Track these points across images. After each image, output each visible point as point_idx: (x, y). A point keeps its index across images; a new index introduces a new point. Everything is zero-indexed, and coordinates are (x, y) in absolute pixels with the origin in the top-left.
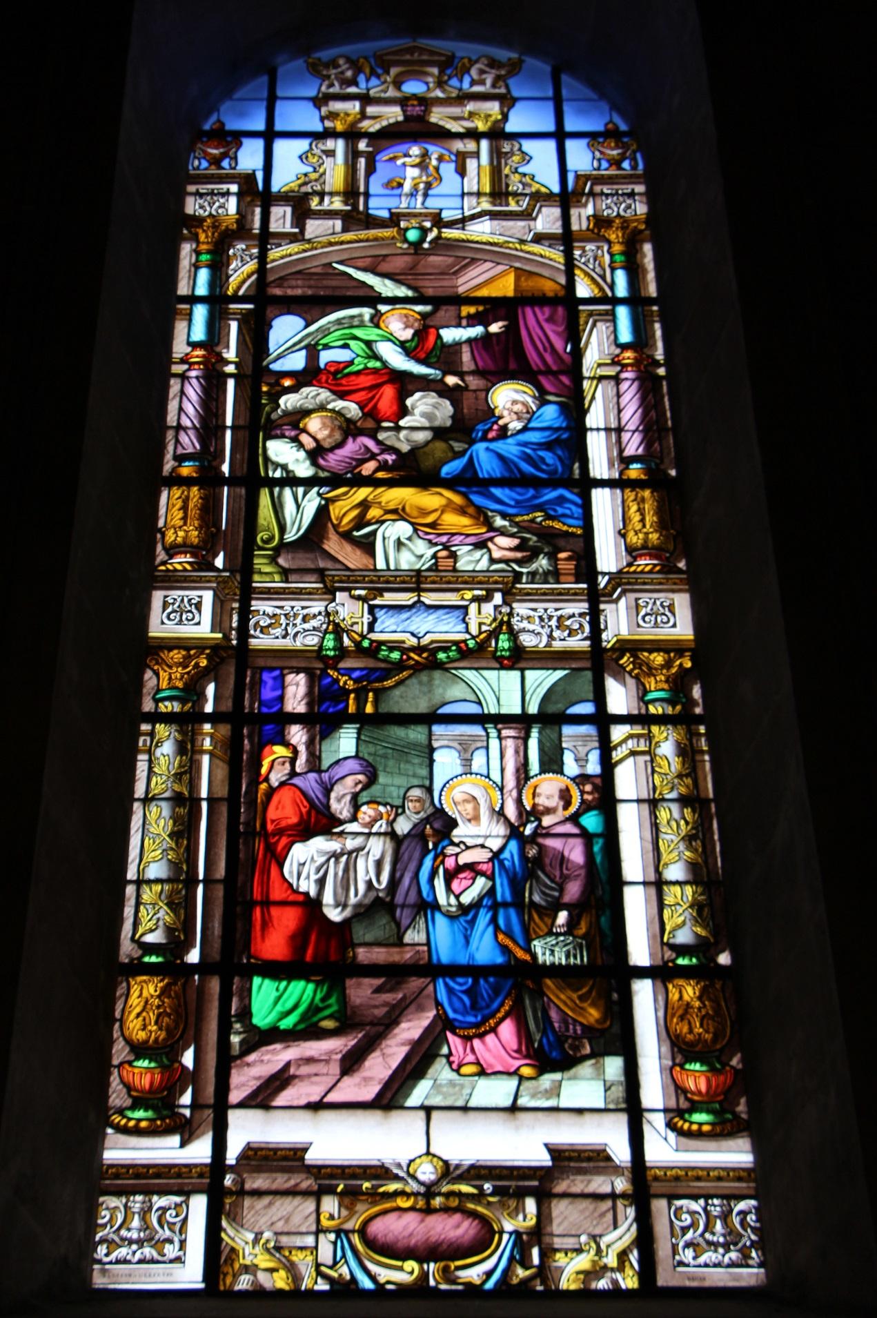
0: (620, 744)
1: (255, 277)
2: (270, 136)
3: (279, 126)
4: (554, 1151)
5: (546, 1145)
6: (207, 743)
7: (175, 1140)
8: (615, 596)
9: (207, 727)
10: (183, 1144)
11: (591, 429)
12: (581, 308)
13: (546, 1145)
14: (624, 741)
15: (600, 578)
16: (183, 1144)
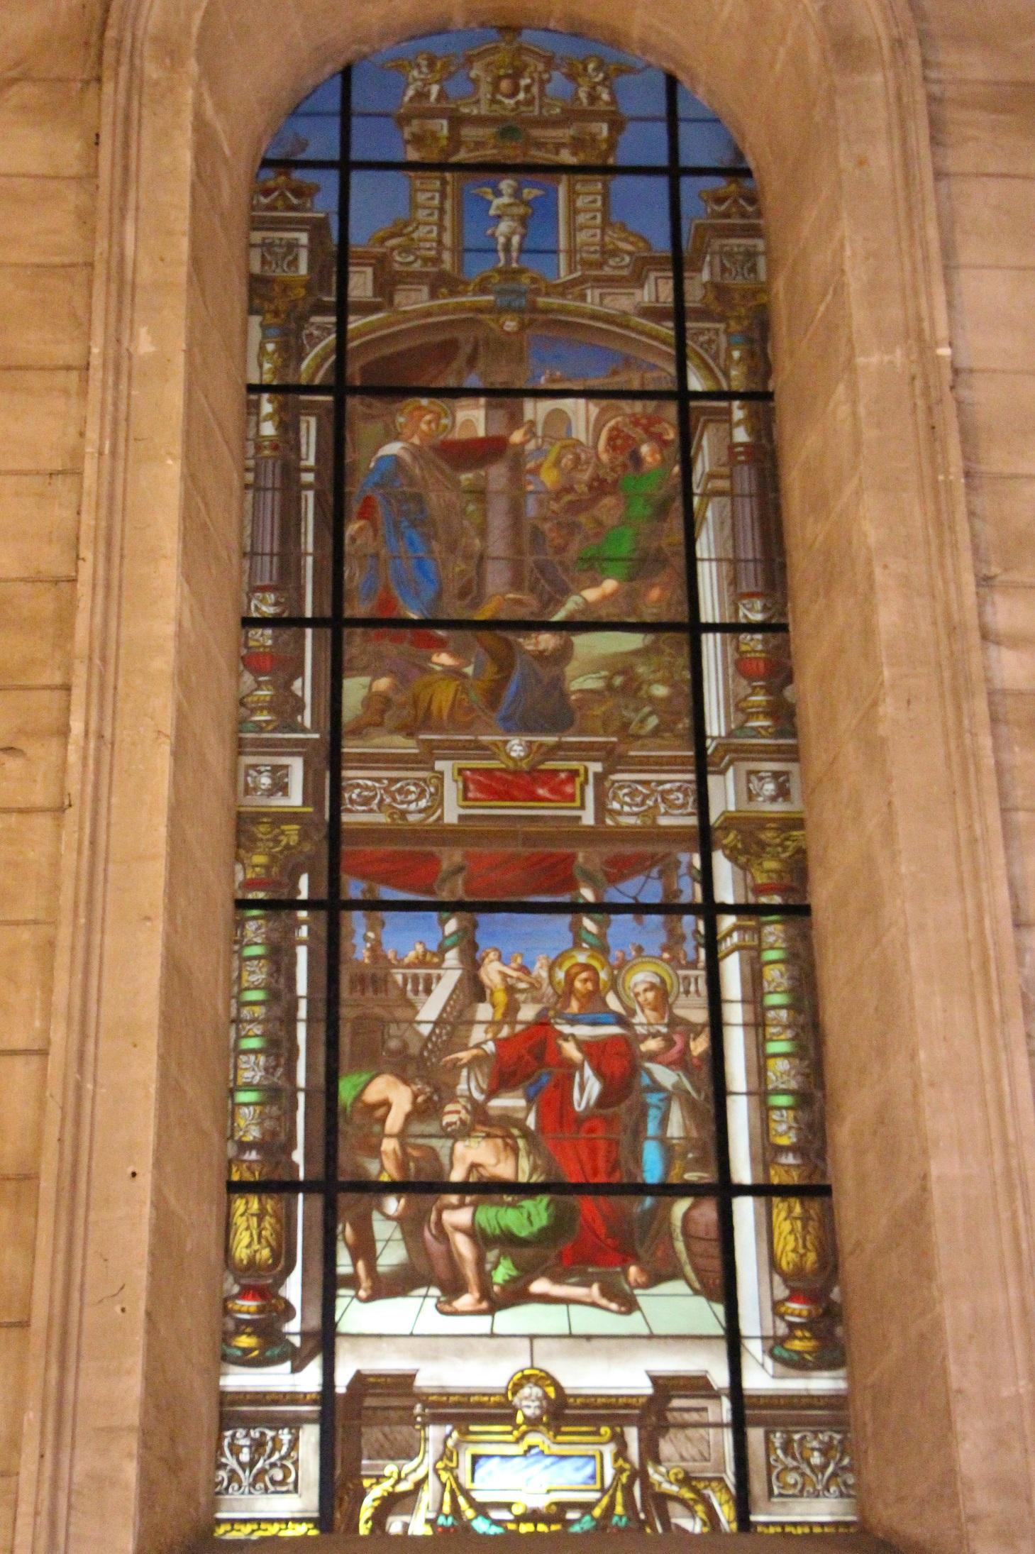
0: (724, 938)
1: (333, 358)
2: (345, 166)
3: (355, 155)
4: (655, 1380)
5: (647, 1372)
6: (304, 932)
7: (287, 1366)
8: (723, 765)
9: (303, 914)
10: (295, 1370)
11: (703, 560)
12: (693, 404)
13: (647, 1372)
14: (729, 934)
15: (708, 742)
16: (295, 1370)
